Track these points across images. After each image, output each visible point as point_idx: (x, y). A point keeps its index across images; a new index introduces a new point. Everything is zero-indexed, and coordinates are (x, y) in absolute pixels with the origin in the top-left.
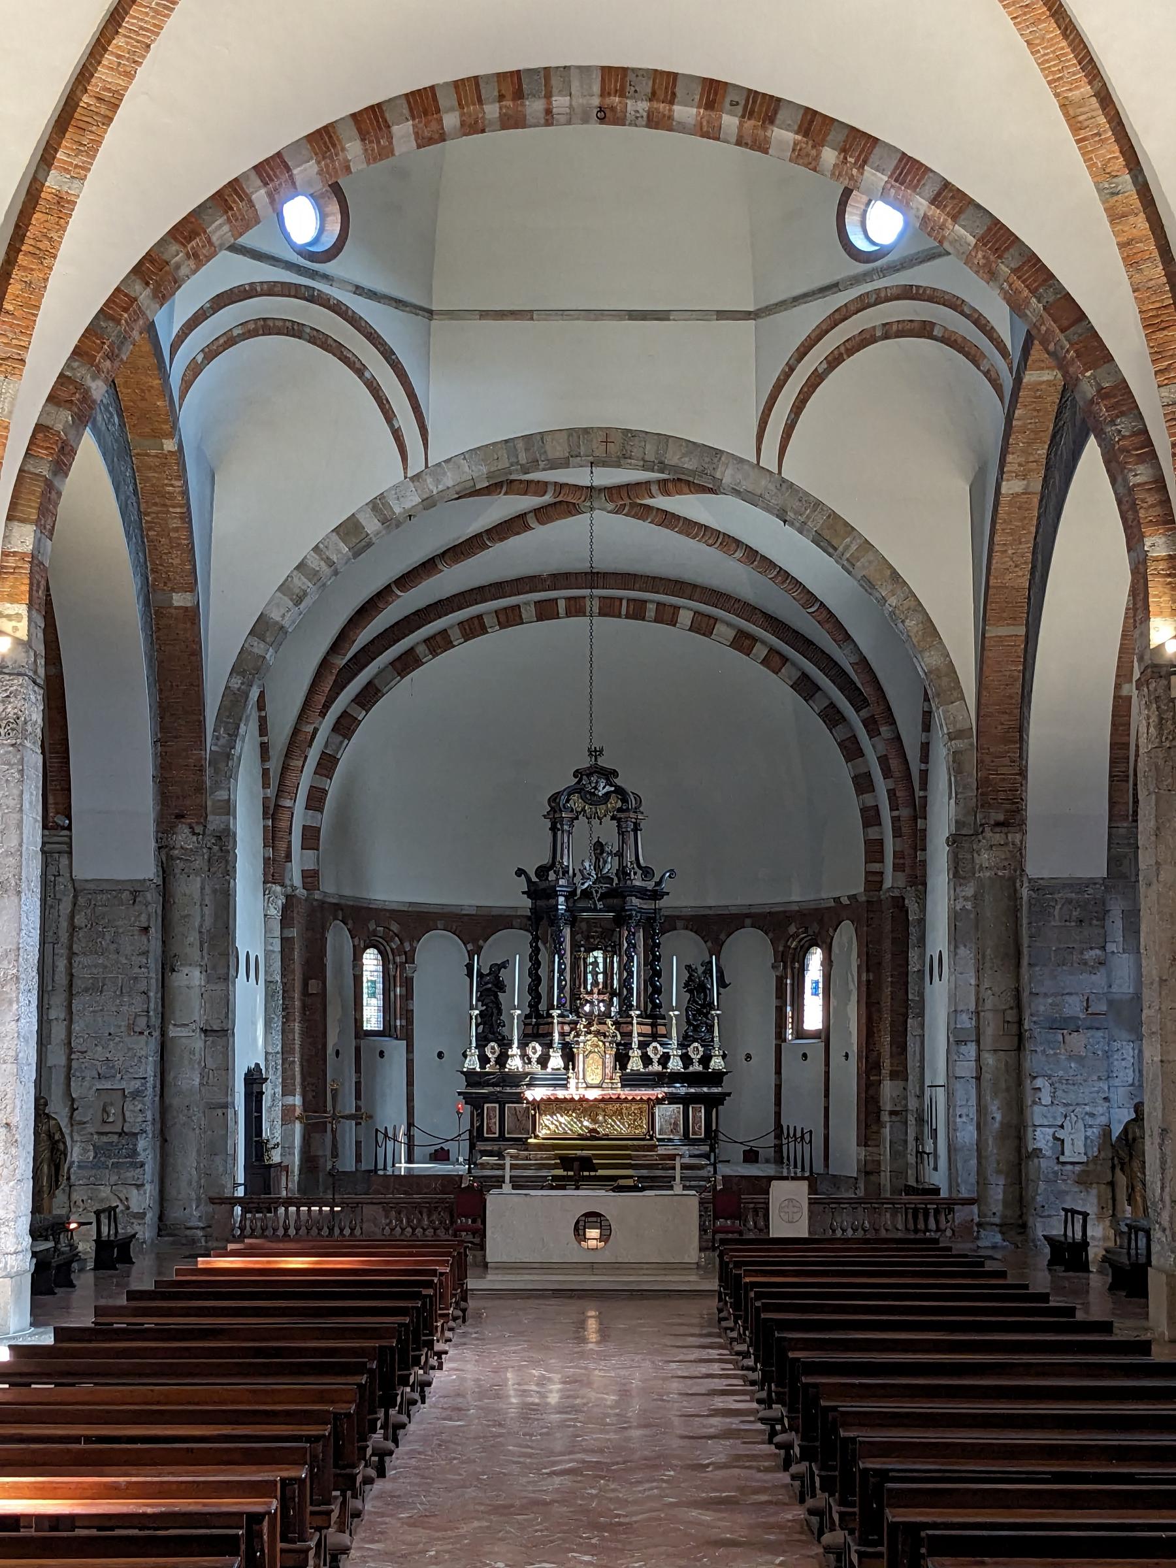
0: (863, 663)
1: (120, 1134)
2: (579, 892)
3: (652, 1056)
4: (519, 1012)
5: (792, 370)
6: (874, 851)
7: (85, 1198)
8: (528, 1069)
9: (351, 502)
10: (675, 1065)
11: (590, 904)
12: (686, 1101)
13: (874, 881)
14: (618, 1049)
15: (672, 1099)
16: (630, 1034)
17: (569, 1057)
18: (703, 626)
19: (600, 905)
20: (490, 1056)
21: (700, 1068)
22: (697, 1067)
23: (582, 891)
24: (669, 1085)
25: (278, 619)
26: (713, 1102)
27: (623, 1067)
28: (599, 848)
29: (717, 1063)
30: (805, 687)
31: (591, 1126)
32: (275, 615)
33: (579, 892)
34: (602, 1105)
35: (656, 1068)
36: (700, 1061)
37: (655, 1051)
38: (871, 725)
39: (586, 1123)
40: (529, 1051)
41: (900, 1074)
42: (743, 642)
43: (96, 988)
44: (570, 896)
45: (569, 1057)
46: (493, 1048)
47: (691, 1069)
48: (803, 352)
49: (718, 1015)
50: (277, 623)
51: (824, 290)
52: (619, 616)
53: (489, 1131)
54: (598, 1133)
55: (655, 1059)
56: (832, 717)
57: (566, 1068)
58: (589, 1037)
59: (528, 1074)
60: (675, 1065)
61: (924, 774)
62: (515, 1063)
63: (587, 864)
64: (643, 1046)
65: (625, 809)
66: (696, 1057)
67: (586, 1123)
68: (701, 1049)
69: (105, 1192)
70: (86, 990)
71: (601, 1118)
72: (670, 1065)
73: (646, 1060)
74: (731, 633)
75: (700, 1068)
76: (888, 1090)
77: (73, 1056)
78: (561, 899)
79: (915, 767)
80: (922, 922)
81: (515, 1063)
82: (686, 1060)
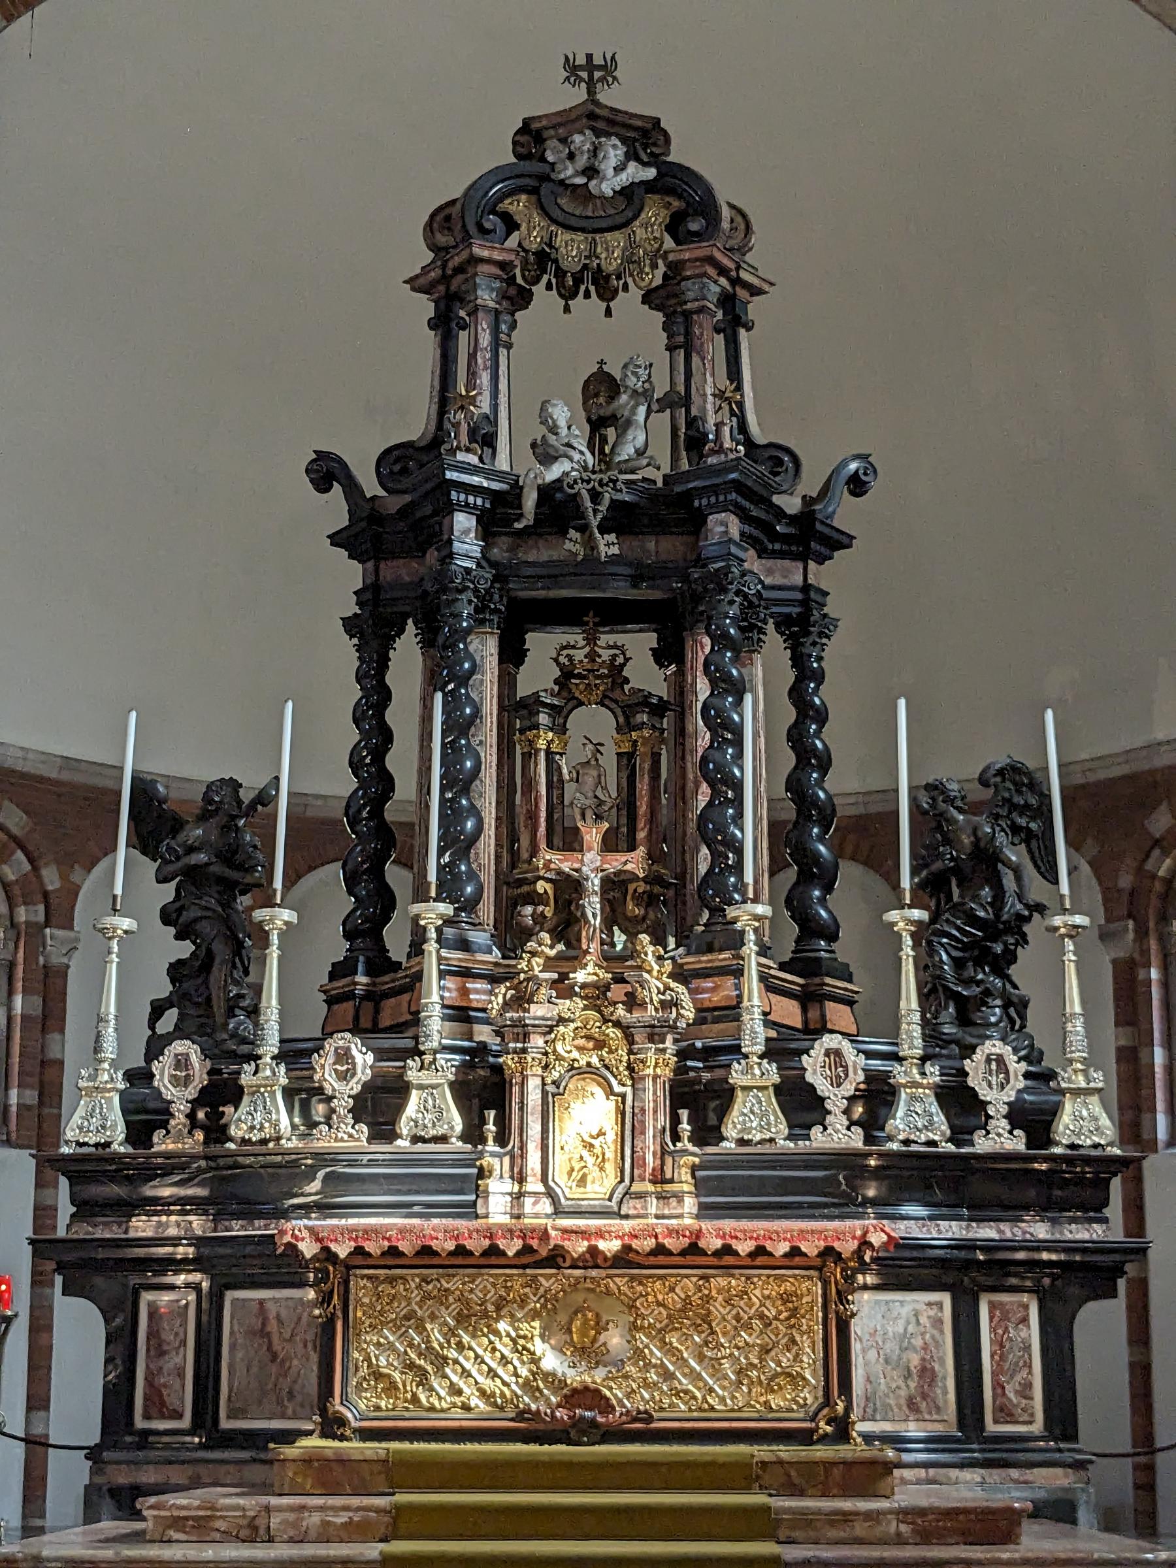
2: (530, 500)
3: (823, 1087)
4: (287, 915)
8: (323, 1140)
10: (917, 1121)
11: (573, 544)
12: (963, 1276)
14: (680, 1070)
15: (904, 1269)
16: (732, 1011)
17: (486, 1091)
19: (608, 546)
20: (169, 1092)
21: (1017, 1143)
22: (1000, 1139)
23: (547, 492)
24: (884, 1205)
27: (707, 1133)
28: (601, 387)
29: (1086, 1123)
31: (575, 1377)
33: (530, 500)
34: (619, 1282)
35: (838, 1134)
36: (1017, 1116)
37: (834, 1066)
39: (551, 1361)
40: (325, 1071)
44: (497, 514)
45: (486, 1091)
46: (182, 1062)
47: (982, 1144)
49: (1075, 932)
53: (157, 1405)
54: (606, 1406)
55: (835, 1098)
57: (473, 1135)
58: (565, 1006)
59: (323, 1158)
60: (917, 1121)
62: (264, 1116)
63: (561, 414)
64: (784, 1049)
65: (687, 244)
66: (997, 1099)
67: (551, 1361)
68: (1018, 1068)
71: (614, 1339)
72: (899, 1123)
73: (802, 1105)
75: (1017, 1143)
78: (463, 522)
81: (264, 1116)
82: (960, 1102)
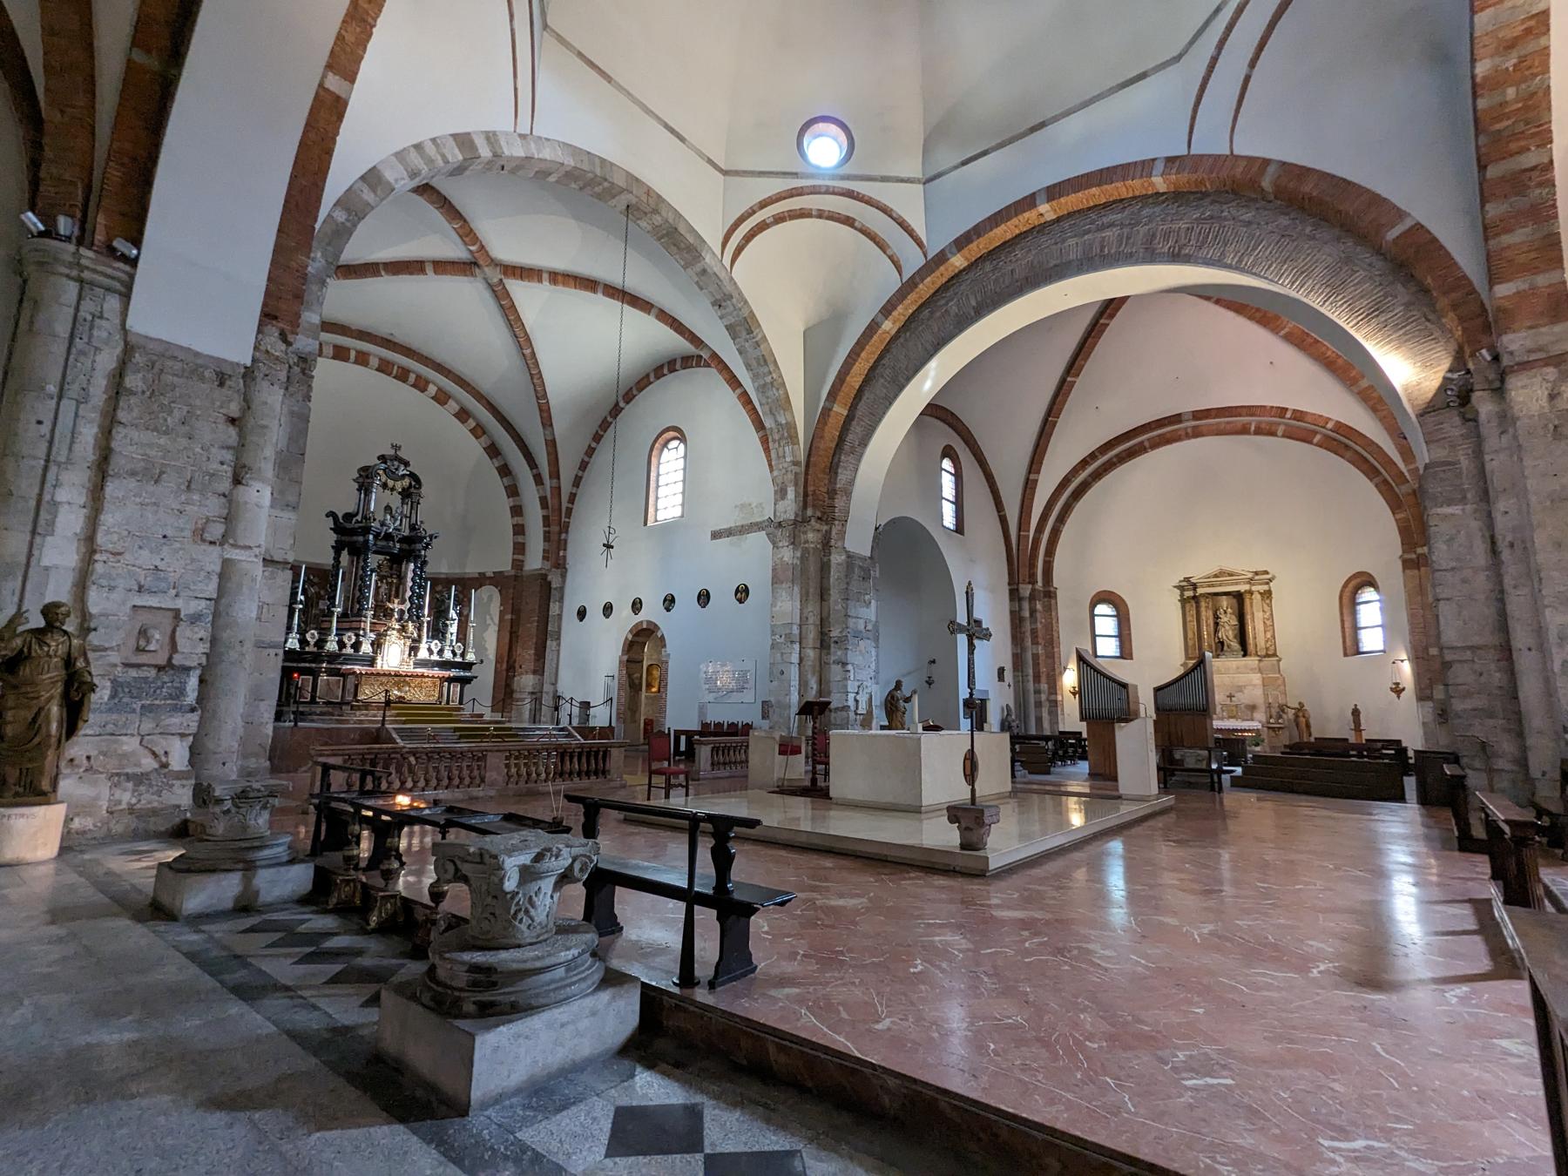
0: (552, 445)
1: (160, 668)
5: (754, 212)
6: (520, 548)
7: (93, 753)
9: (473, 124)
13: (518, 564)
18: (442, 398)
25: (391, 180)
26: (464, 681)
30: (493, 451)
32: (389, 175)
38: (538, 479)
41: (539, 671)
42: (463, 415)
43: (152, 474)
48: (763, 205)
50: (389, 183)
51: (785, 174)
52: (389, 375)
56: (505, 471)
61: (569, 512)
69: (130, 744)
70: (133, 474)
74: (457, 408)
76: (526, 681)
77: (97, 557)
79: (565, 505)
80: (562, 589)
